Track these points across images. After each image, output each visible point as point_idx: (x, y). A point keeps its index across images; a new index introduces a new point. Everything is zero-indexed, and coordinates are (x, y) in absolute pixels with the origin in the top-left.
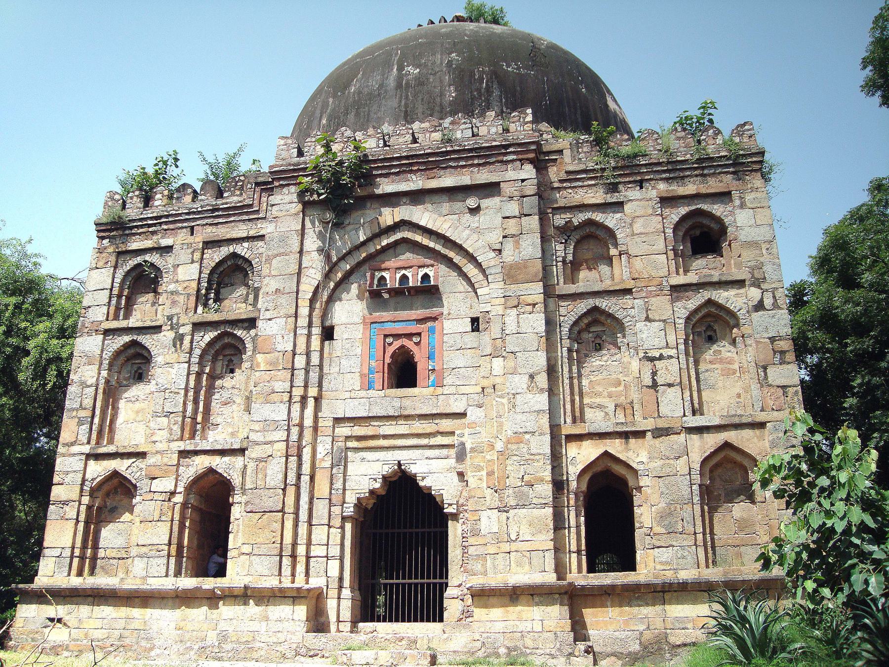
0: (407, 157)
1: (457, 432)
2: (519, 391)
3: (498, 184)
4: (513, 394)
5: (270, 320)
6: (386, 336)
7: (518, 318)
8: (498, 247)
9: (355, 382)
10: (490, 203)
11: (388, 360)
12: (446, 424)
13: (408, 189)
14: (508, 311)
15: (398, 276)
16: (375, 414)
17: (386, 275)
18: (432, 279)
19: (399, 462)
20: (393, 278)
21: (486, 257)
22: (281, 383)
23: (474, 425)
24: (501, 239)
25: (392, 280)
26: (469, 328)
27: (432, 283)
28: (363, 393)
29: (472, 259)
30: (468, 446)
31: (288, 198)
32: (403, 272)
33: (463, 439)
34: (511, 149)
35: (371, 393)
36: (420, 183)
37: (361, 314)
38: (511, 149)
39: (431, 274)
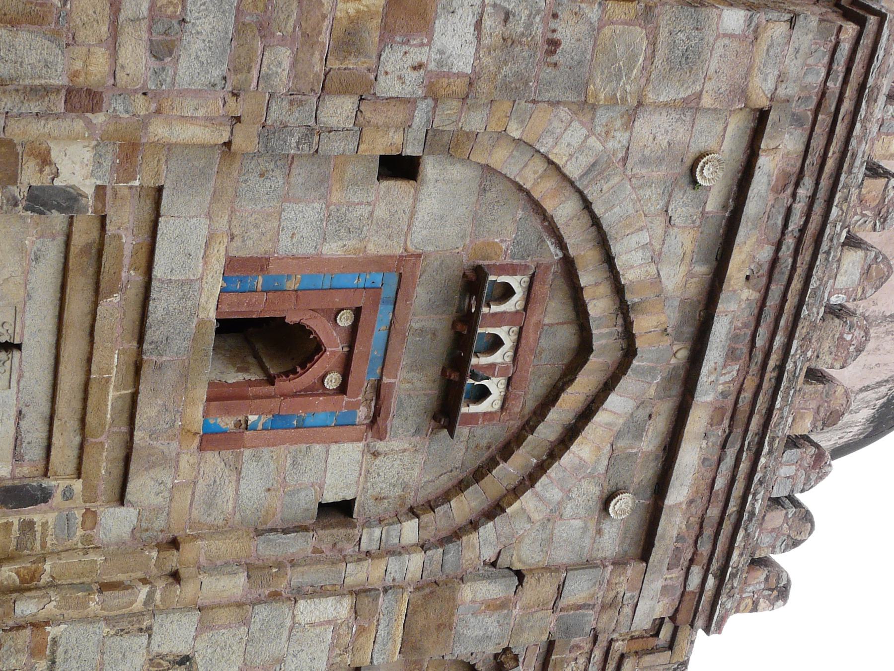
0: (781, 369)
1: (78, 485)
2: (156, 639)
3: (645, 555)
4: (149, 629)
5: (478, 25)
6: (357, 312)
7: (329, 622)
8: (503, 561)
9: (252, 246)
10: (612, 539)
11: (292, 319)
12: (103, 464)
13: (704, 370)
14: (347, 602)
15: (501, 332)
16: (154, 295)
17: (513, 304)
18: (474, 409)
19: (19, 347)
20: (499, 319)
21: (485, 542)
22: (286, 64)
23: (88, 524)
24: (517, 566)
25: (498, 321)
26: (330, 497)
27: (464, 410)
28: (217, 265)
29: (494, 511)
30: (38, 515)
31: (793, 66)
32: (508, 342)
33: (57, 498)
34: (711, 582)
35: (214, 284)
36: (709, 398)
37: (430, 249)
38: (711, 582)
39: (485, 406)
